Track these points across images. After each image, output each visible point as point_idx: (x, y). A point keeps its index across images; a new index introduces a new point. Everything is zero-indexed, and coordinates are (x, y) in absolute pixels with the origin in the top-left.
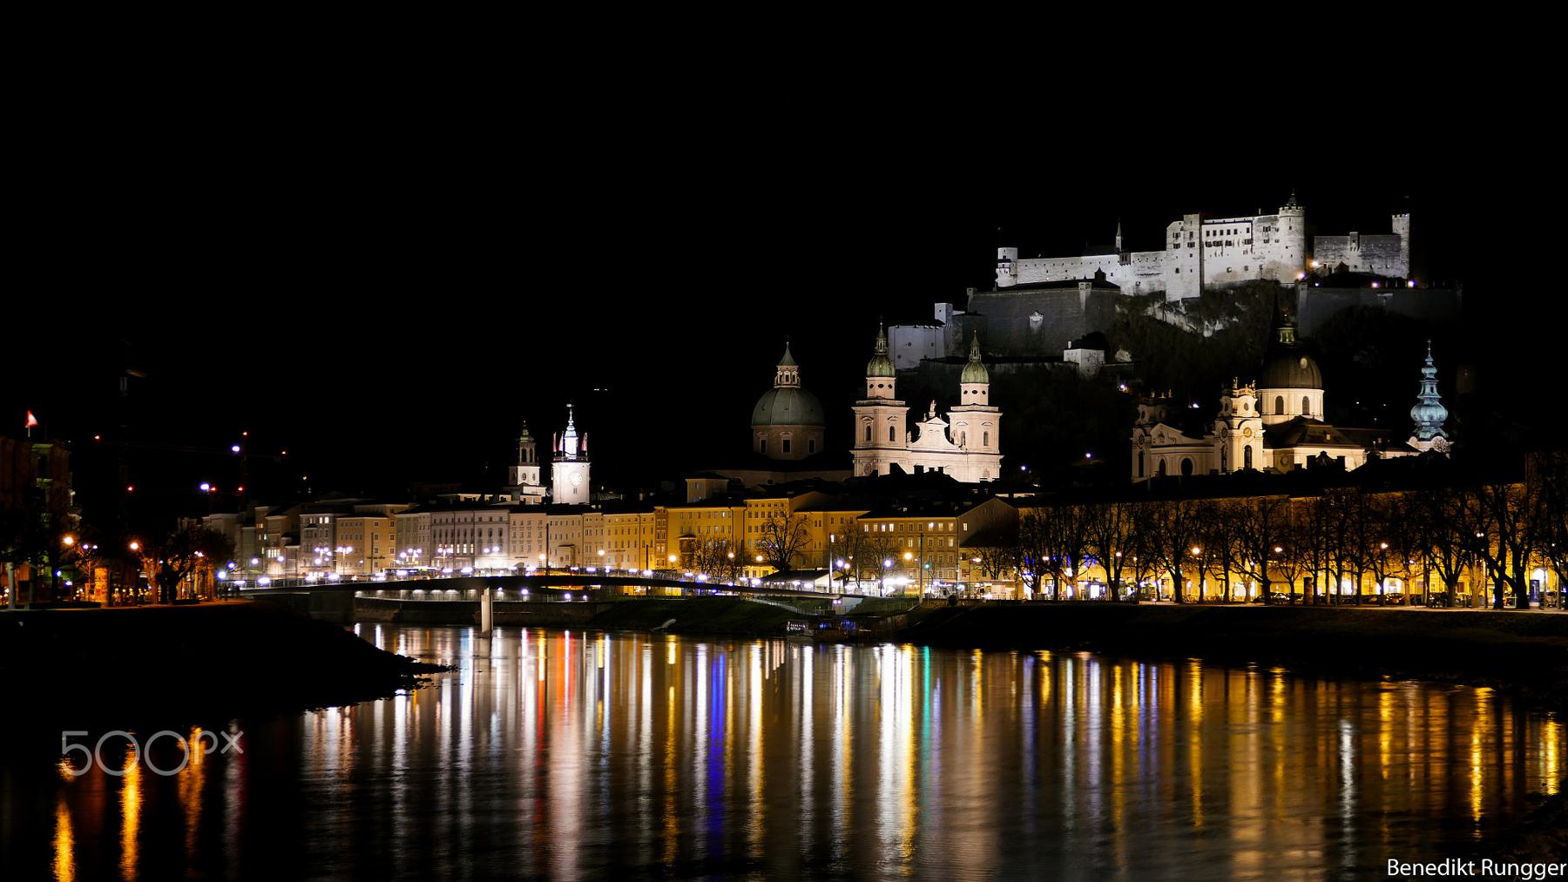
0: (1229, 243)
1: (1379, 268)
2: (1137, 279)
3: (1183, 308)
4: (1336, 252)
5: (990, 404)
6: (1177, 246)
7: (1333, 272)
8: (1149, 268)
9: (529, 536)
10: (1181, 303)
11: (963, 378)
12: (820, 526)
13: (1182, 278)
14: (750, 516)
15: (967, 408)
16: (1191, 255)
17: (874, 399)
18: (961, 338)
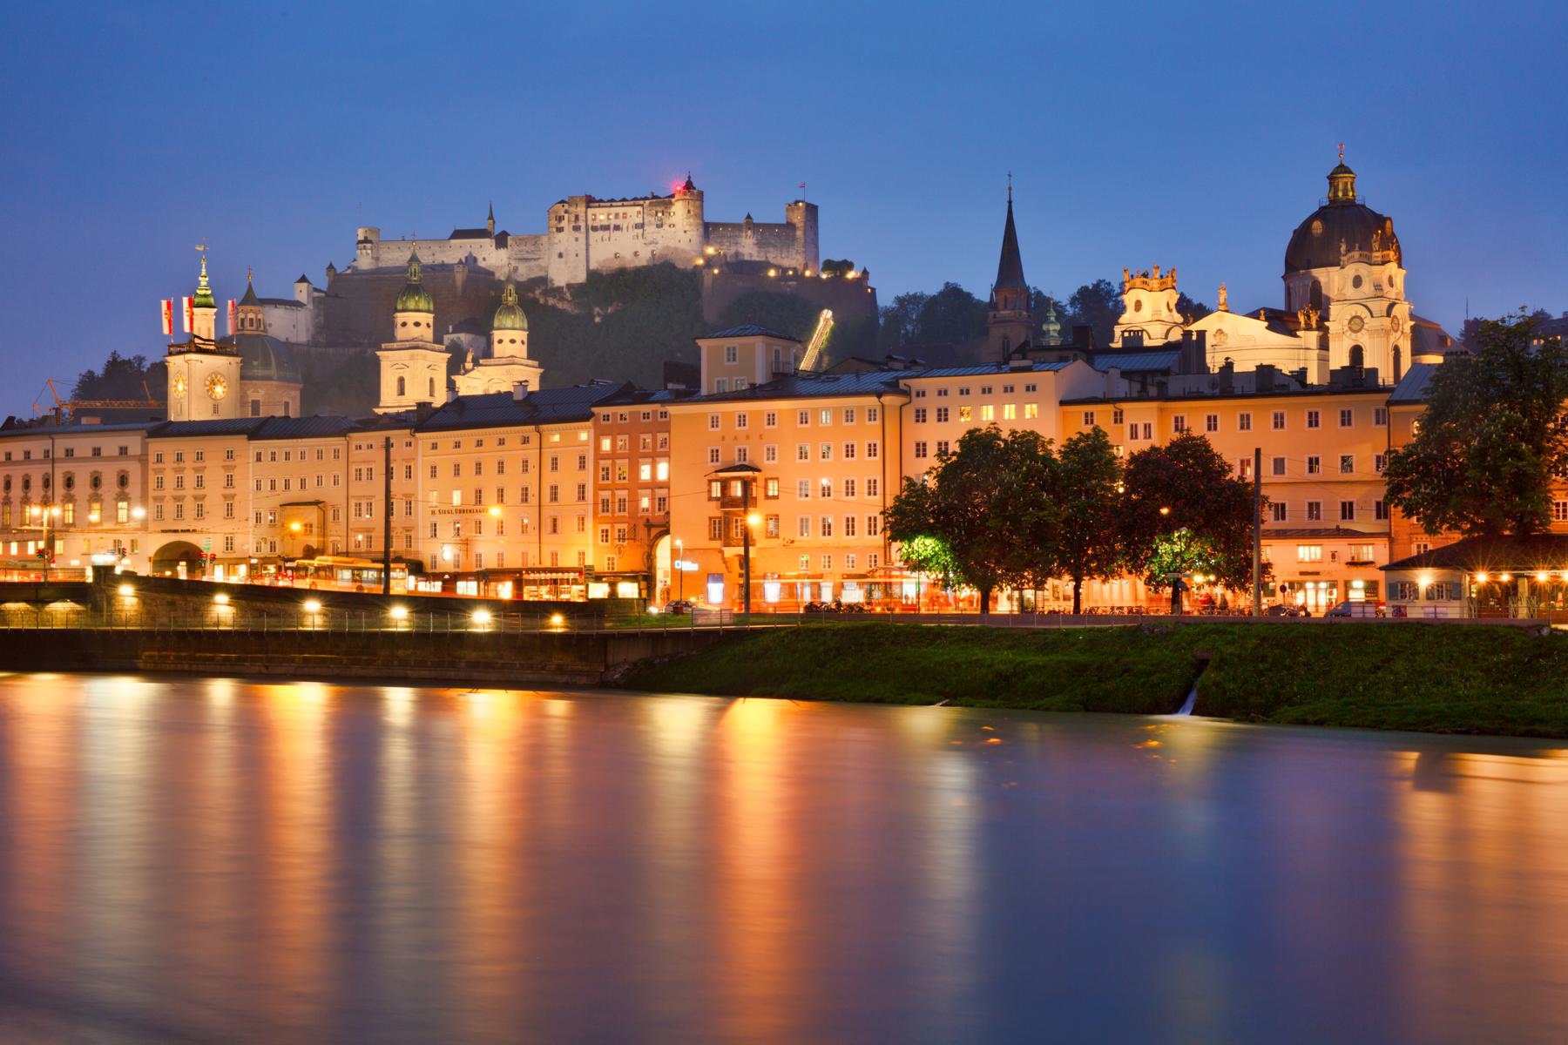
0: (617, 228)
1: (773, 256)
2: (514, 264)
3: (568, 294)
4: (732, 241)
5: (530, 357)
6: (560, 230)
7: (728, 259)
8: (527, 252)
9: (200, 483)
10: (565, 290)
11: (496, 324)
12: (1148, 436)
13: (566, 263)
14: (921, 416)
15: (504, 361)
16: (577, 239)
17: (407, 341)
18: (322, 322)
